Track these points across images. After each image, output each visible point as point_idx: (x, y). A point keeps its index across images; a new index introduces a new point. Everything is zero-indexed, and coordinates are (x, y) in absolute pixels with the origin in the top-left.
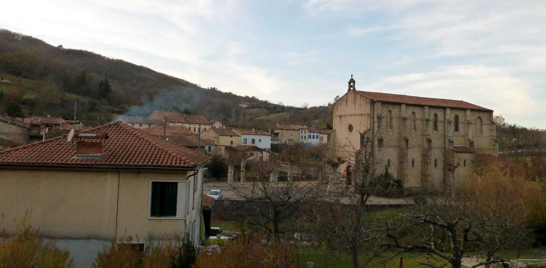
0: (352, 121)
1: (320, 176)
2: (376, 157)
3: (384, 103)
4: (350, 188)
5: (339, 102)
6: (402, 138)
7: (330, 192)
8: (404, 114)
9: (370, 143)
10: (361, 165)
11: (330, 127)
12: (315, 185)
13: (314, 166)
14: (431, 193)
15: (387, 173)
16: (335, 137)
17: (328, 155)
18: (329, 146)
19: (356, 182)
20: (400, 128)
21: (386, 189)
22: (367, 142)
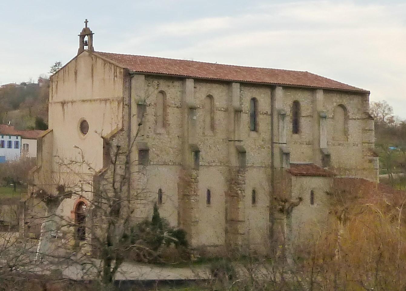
0: (87, 112)
1: (22, 223)
2: (135, 184)
3: (150, 76)
4: (83, 246)
5: (61, 73)
6: (186, 146)
7: (43, 256)
8: (190, 100)
9: (123, 158)
10: (104, 201)
11: (42, 125)
12: (12, 240)
13: (9, 202)
14: (244, 257)
15: (156, 218)
16: (52, 143)
17: (39, 181)
18: (40, 164)
19: (94, 234)
20: (182, 126)
21: (155, 249)
22: (117, 155)
